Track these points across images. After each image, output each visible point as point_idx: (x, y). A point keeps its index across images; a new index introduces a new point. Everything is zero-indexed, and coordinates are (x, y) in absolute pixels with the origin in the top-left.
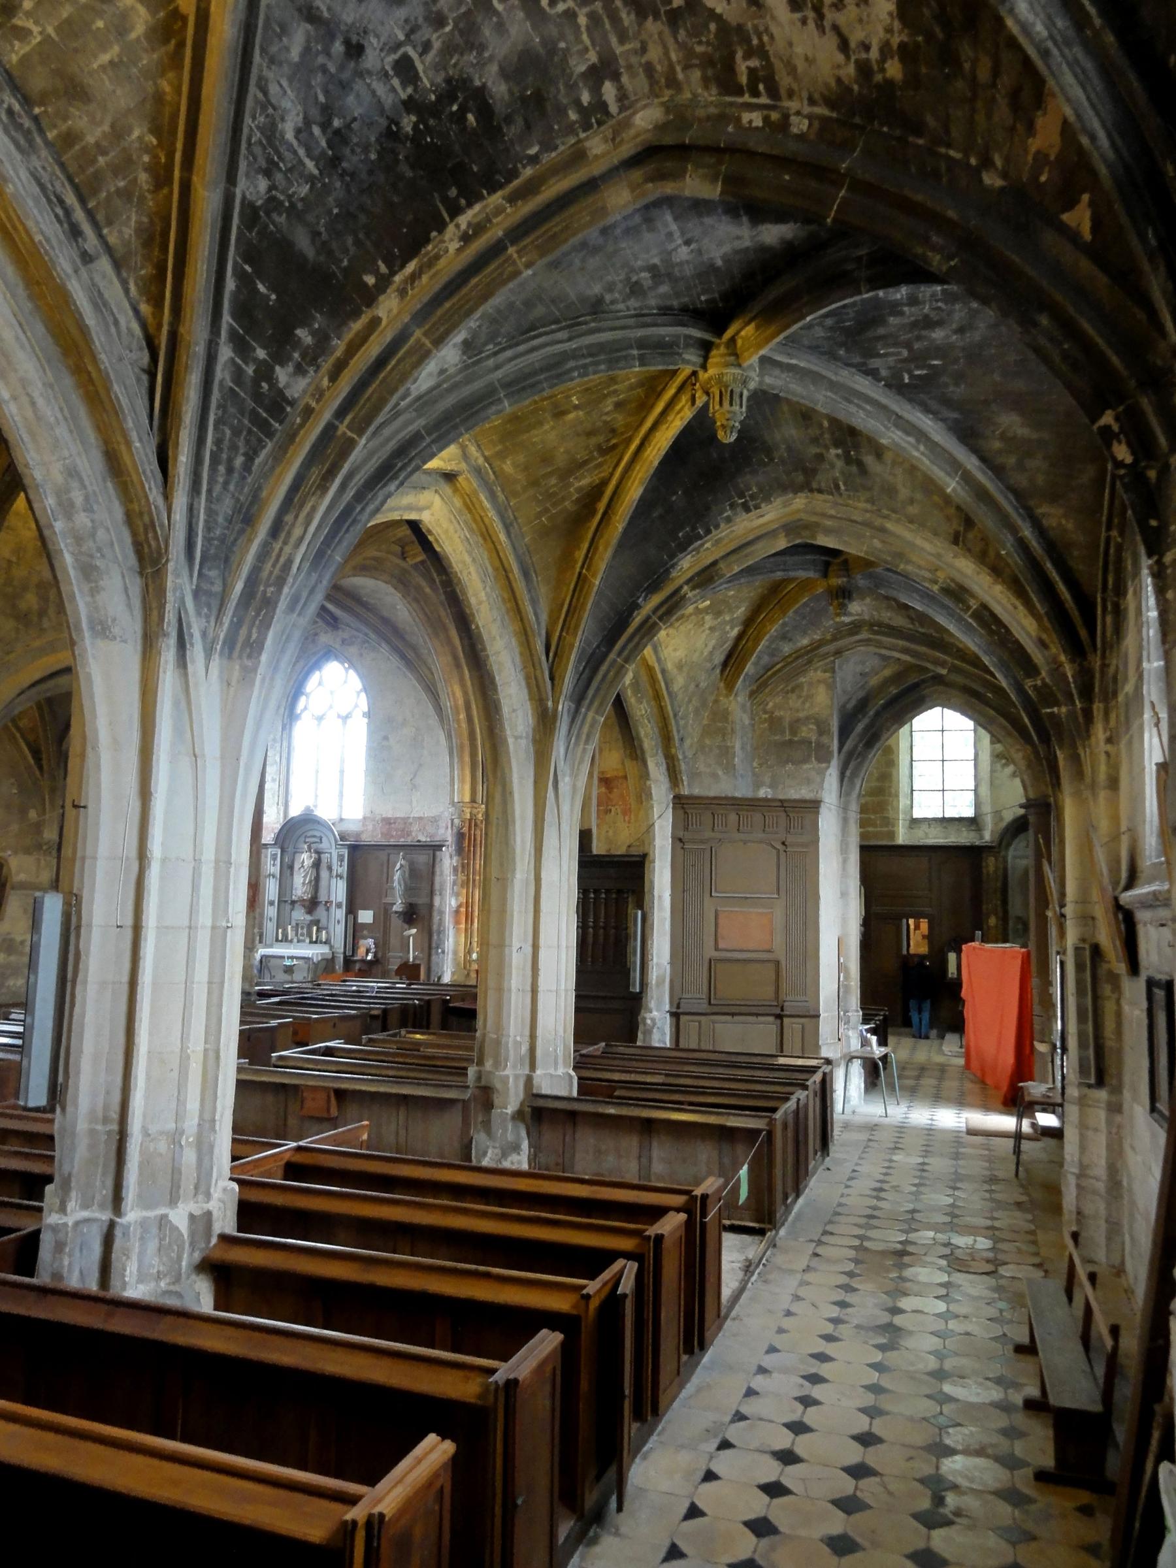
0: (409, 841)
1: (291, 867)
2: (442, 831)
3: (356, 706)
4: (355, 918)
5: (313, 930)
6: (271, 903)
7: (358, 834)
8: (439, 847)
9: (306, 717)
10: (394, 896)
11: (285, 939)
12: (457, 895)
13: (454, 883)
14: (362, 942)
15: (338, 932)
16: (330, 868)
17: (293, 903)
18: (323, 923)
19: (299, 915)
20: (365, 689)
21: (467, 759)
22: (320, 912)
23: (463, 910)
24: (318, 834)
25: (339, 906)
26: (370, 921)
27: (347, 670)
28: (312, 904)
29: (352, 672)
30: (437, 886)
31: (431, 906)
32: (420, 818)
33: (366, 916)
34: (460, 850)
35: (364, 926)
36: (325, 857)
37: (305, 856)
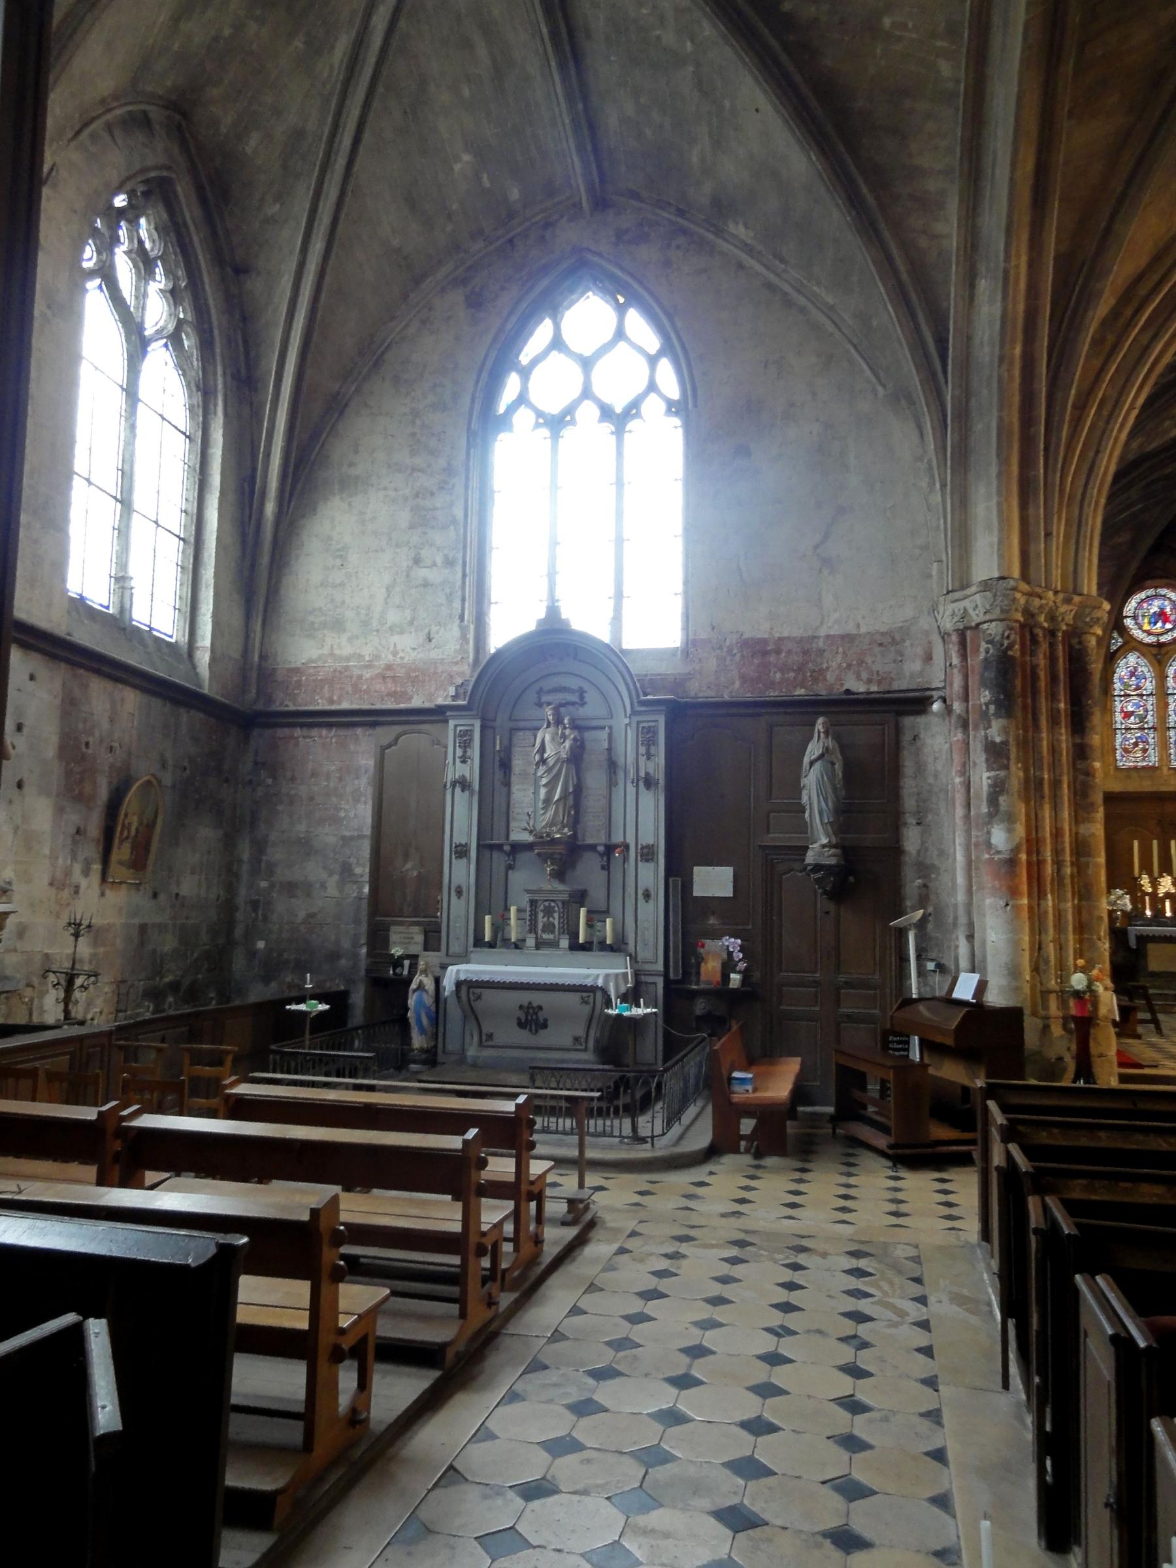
0: (822, 691)
1: (506, 765)
2: (913, 666)
3: (652, 387)
4: (687, 885)
5: (570, 920)
6: (461, 852)
7: (679, 683)
8: (917, 703)
9: (523, 418)
10: (803, 828)
11: (499, 942)
12: (1010, 819)
13: (998, 789)
14: (711, 945)
15: (647, 922)
16: (612, 766)
17: (517, 848)
18: (597, 895)
19: (529, 880)
20: (667, 349)
21: (1015, 469)
22: (589, 872)
23: (1023, 857)
24: (572, 683)
25: (647, 854)
26: (728, 892)
27: (621, 310)
28: (565, 854)
29: (636, 321)
30: (909, 803)
31: (896, 850)
32: (848, 638)
33: (714, 881)
34: (1005, 704)
35: (709, 904)
36: (598, 740)
37: (546, 735)
